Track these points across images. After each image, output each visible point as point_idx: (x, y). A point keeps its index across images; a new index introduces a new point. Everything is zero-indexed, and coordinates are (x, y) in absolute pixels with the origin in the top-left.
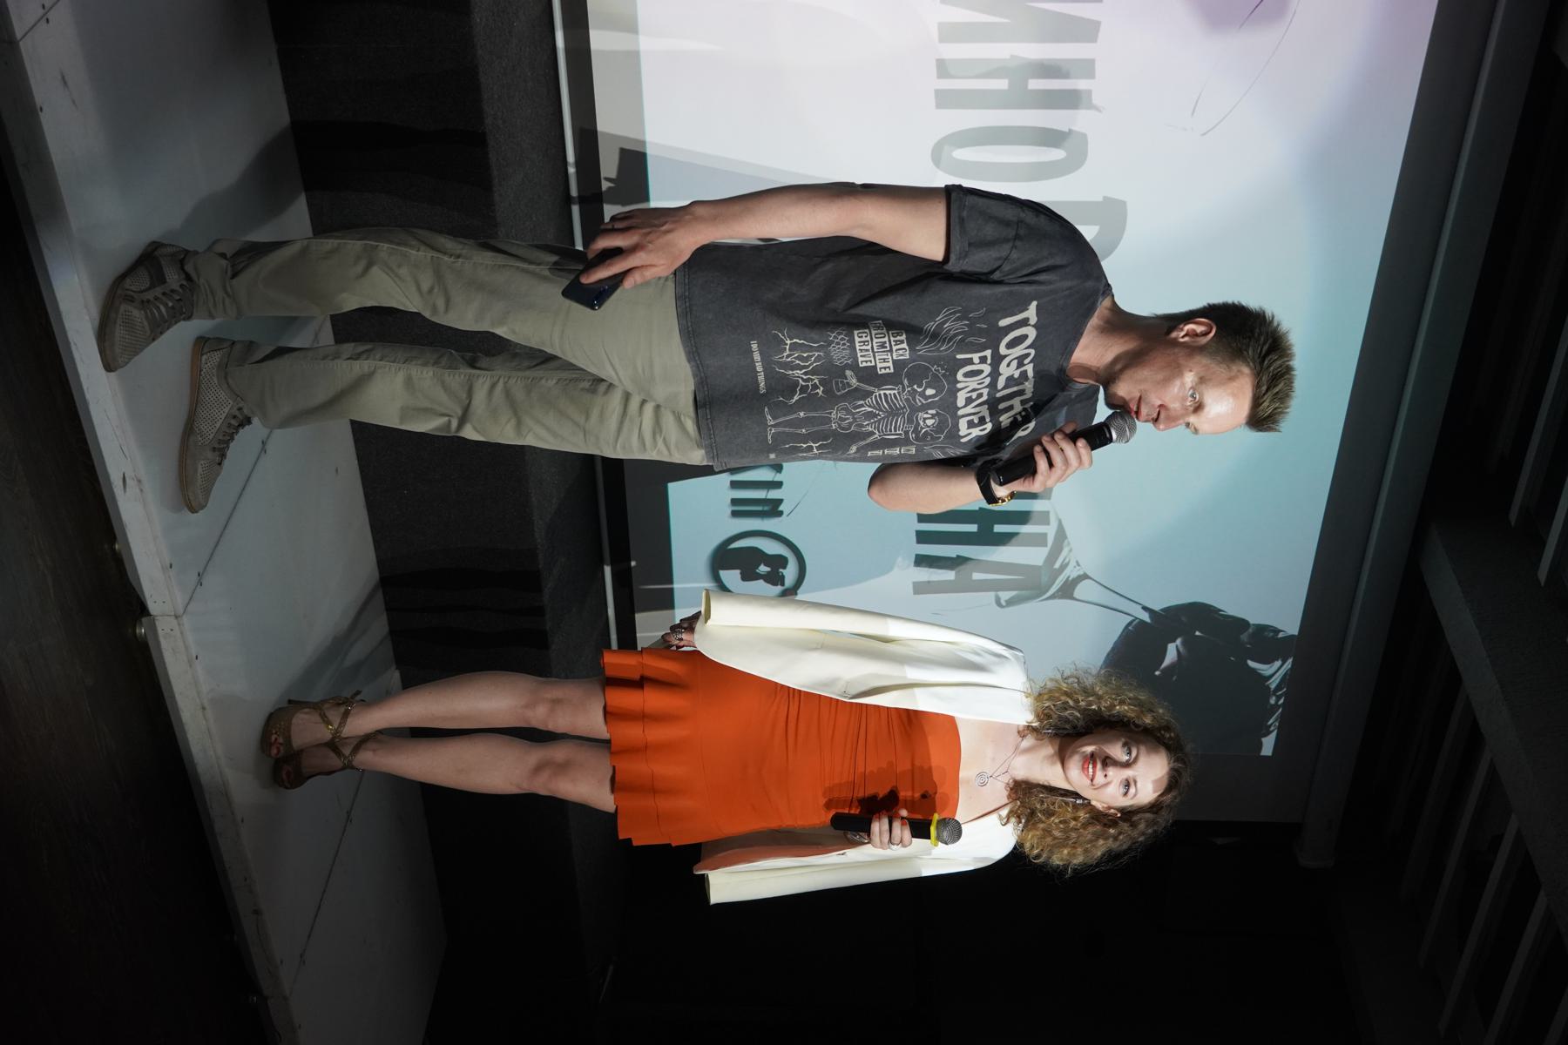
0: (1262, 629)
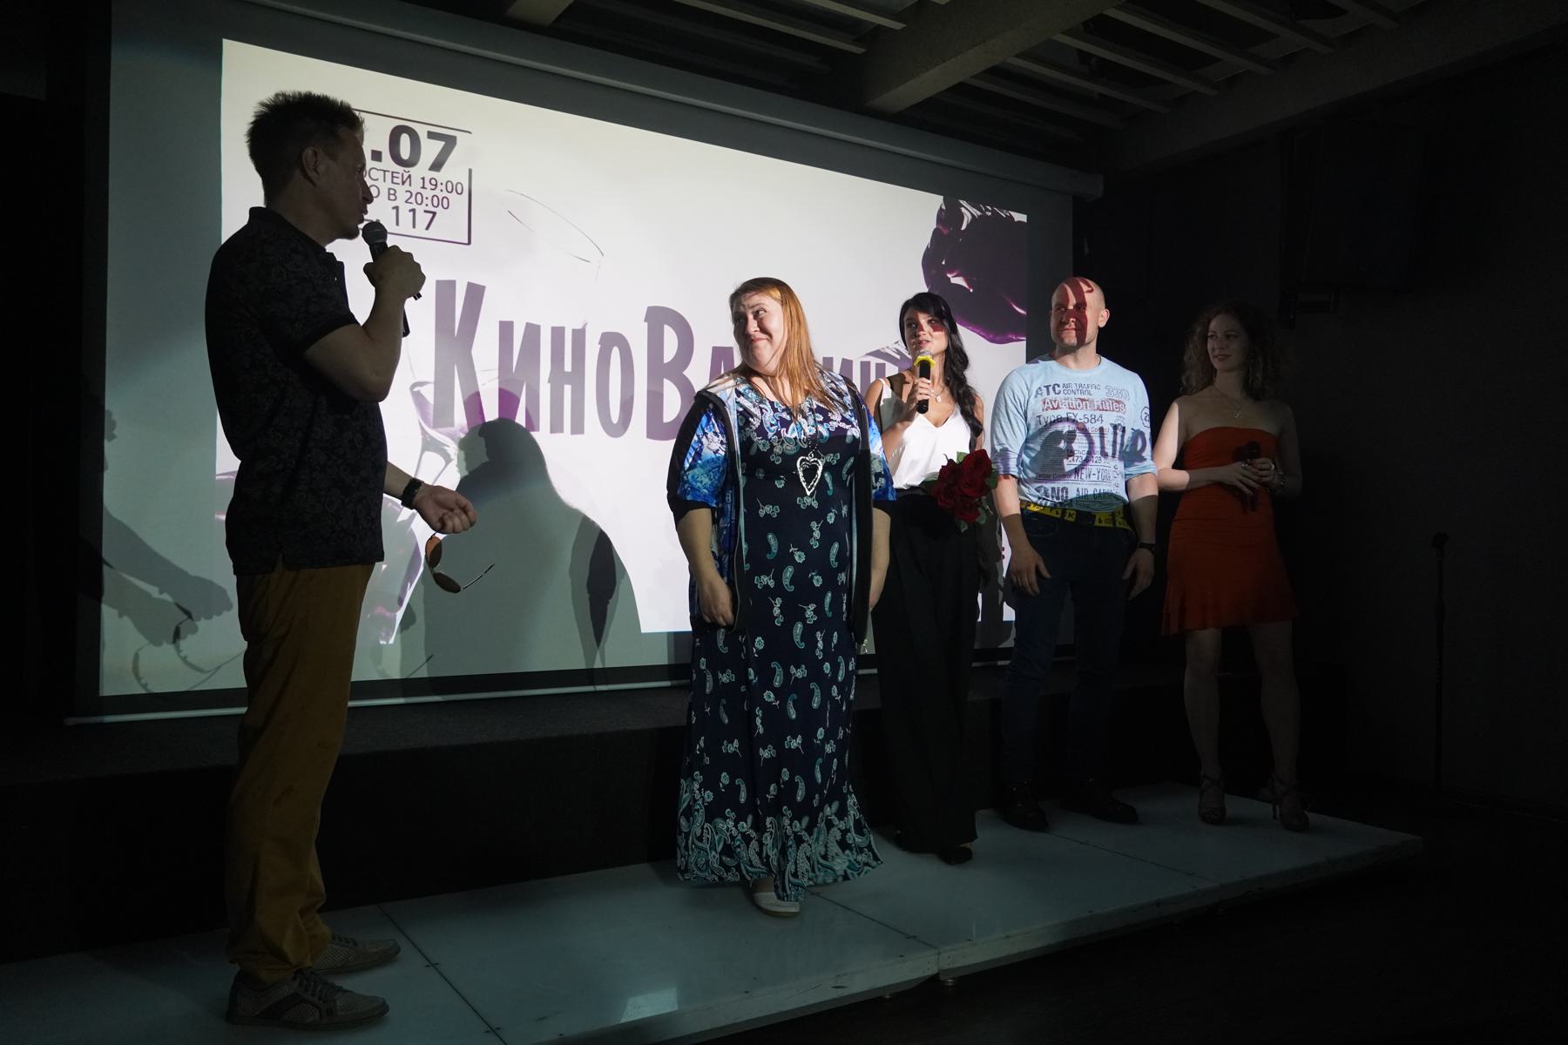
0: (940, 220)
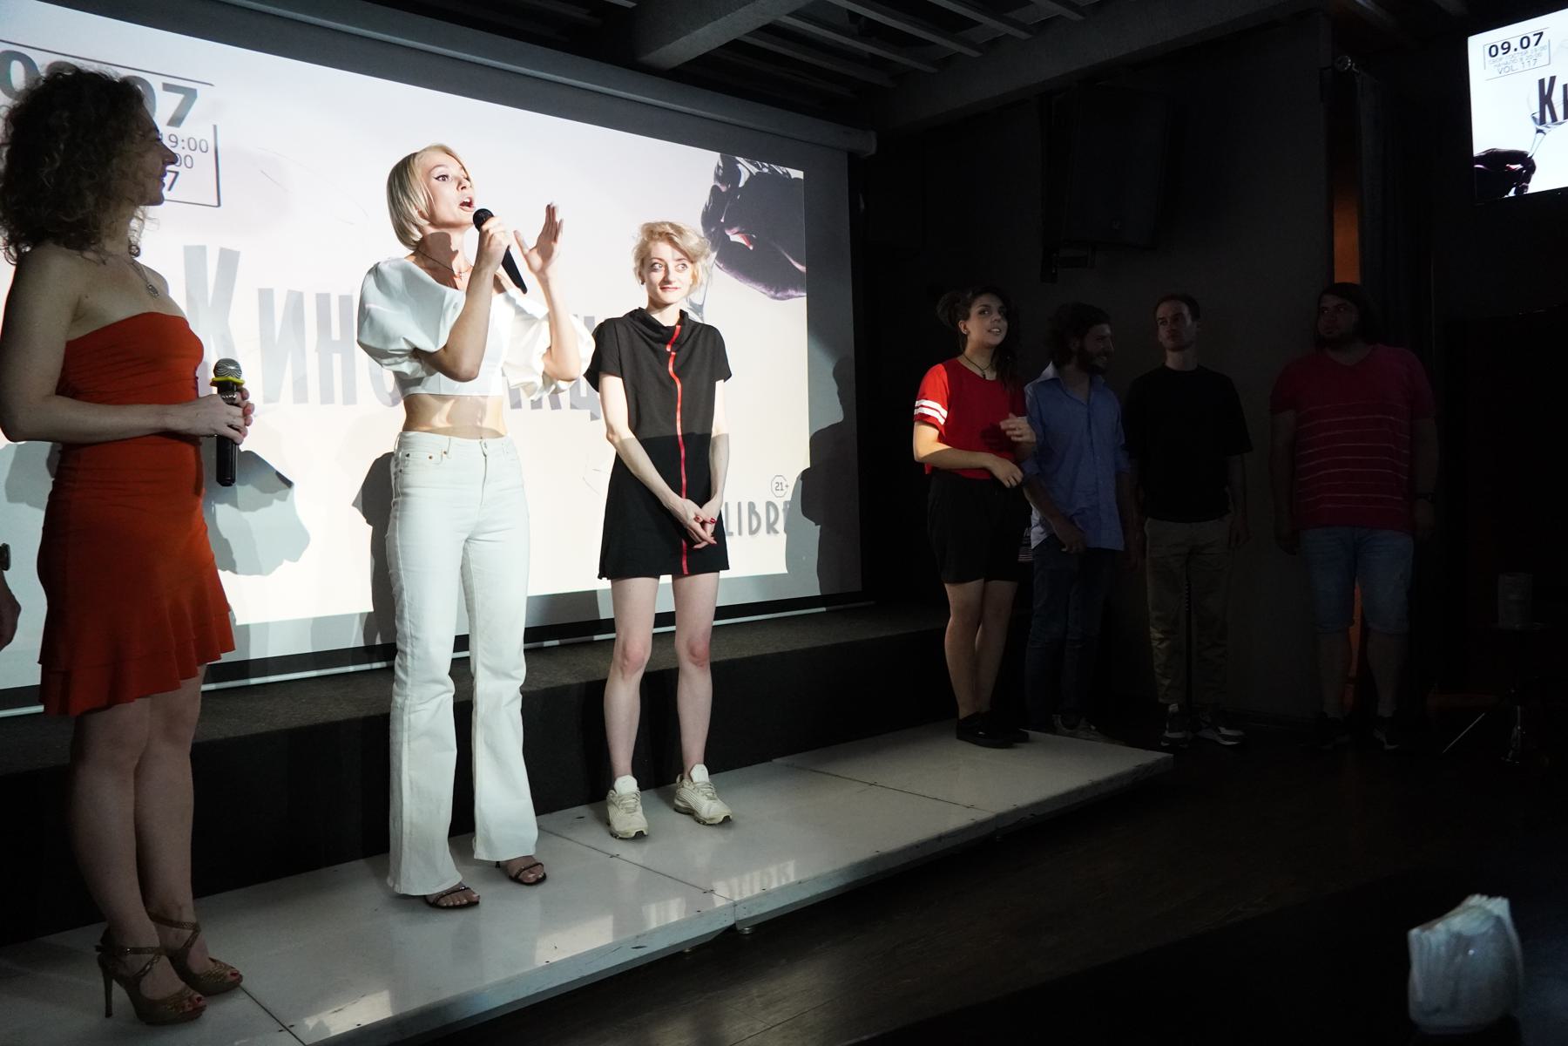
0: (717, 177)
